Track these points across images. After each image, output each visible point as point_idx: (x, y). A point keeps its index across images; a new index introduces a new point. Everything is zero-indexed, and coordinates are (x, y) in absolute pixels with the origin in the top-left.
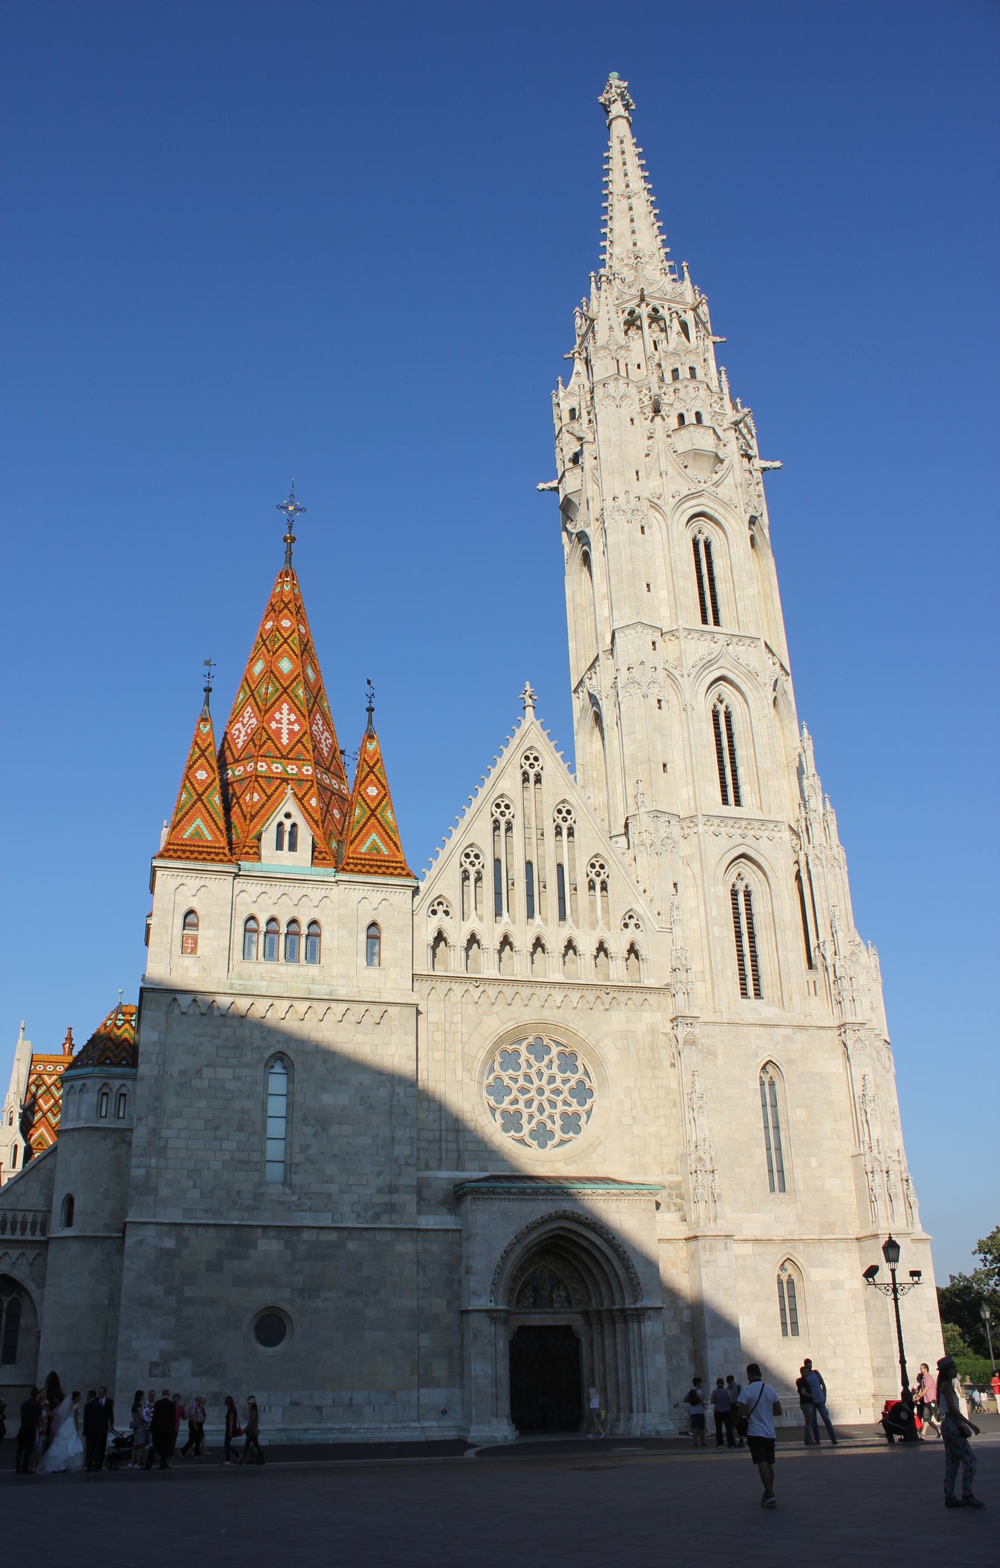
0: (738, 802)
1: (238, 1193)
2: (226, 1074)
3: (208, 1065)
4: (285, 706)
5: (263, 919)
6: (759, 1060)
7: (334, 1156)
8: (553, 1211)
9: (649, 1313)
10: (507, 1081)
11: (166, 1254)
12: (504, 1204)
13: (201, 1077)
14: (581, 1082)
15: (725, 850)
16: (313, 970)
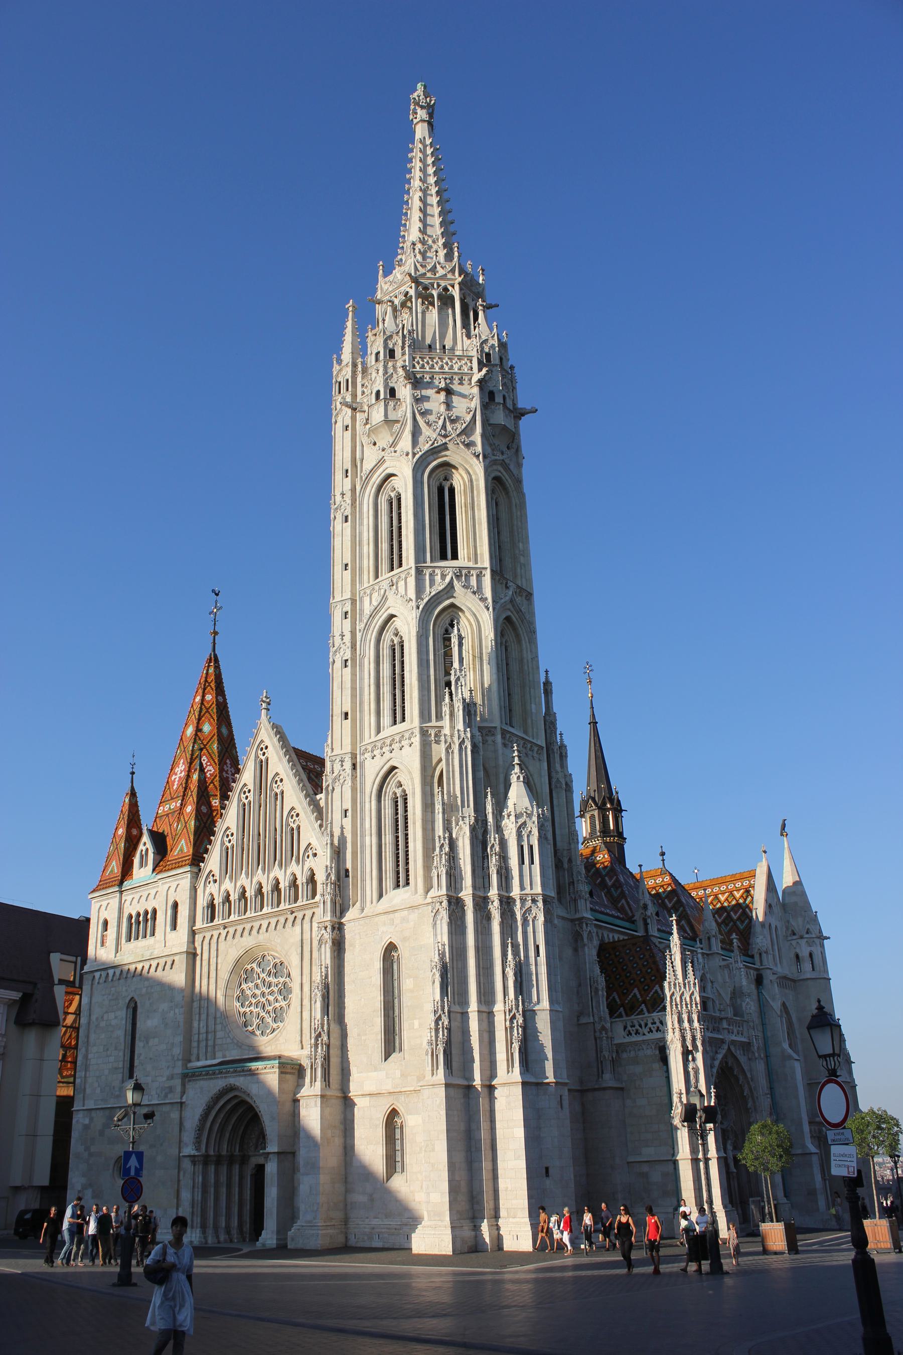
0: (403, 720)
1: (114, 1087)
2: (112, 1015)
3: (107, 1012)
4: (182, 761)
5: (134, 914)
6: (383, 944)
7: (151, 1059)
8: (224, 1085)
9: (271, 1156)
10: (248, 992)
11: (86, 1127)
12: (202, 1082)
13: (103, 1020)
14: (285, 984)
15: (378, 769)
16: (150, 940)
